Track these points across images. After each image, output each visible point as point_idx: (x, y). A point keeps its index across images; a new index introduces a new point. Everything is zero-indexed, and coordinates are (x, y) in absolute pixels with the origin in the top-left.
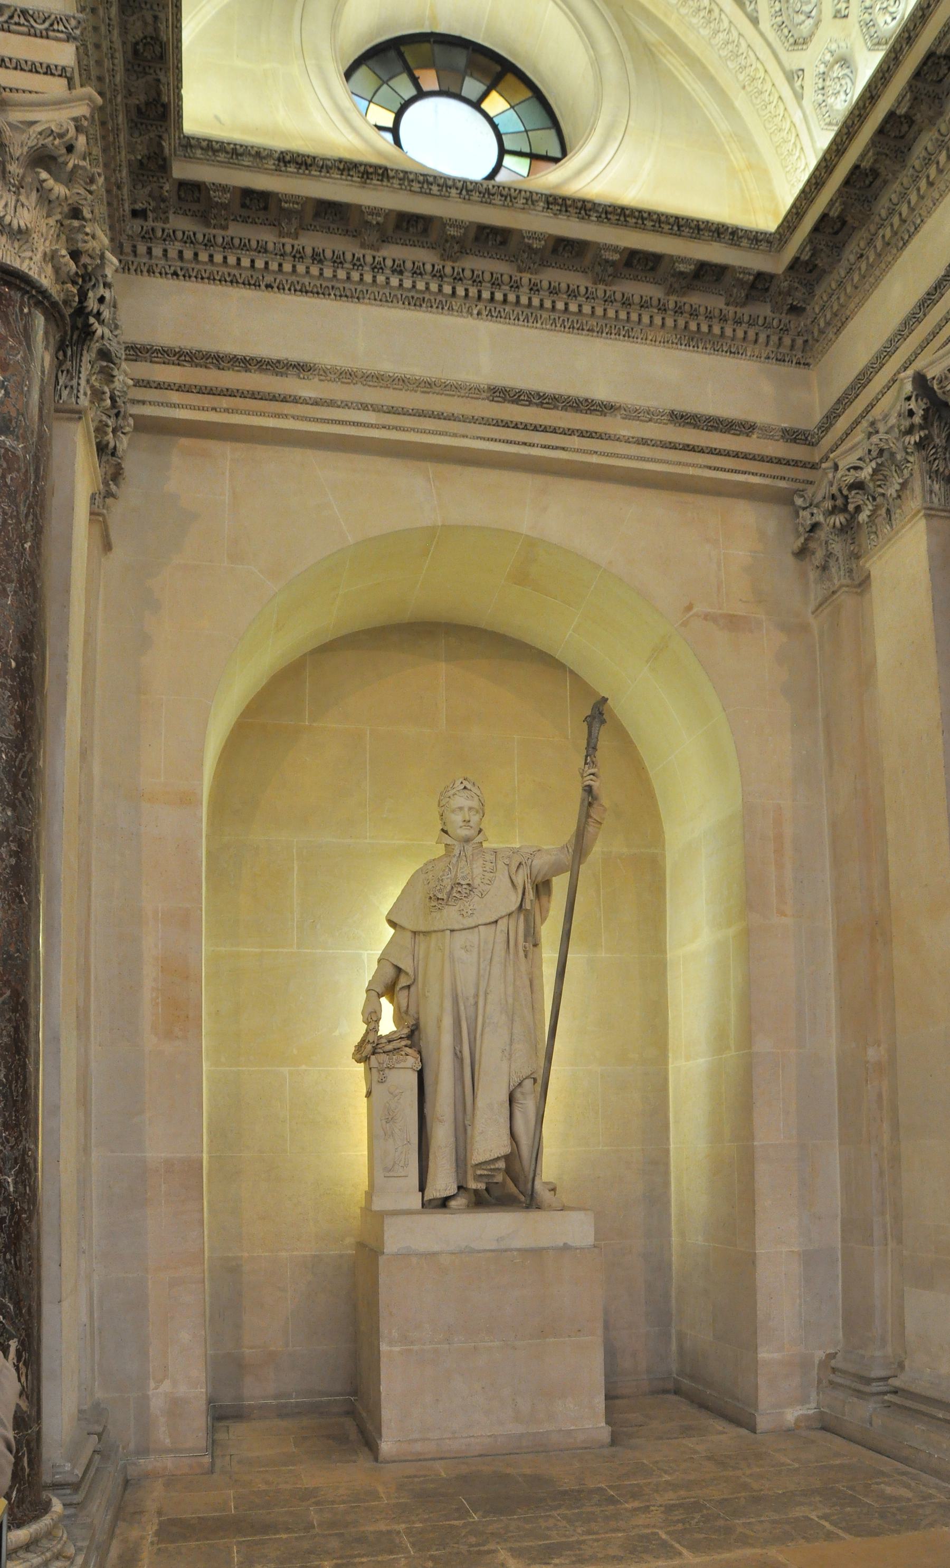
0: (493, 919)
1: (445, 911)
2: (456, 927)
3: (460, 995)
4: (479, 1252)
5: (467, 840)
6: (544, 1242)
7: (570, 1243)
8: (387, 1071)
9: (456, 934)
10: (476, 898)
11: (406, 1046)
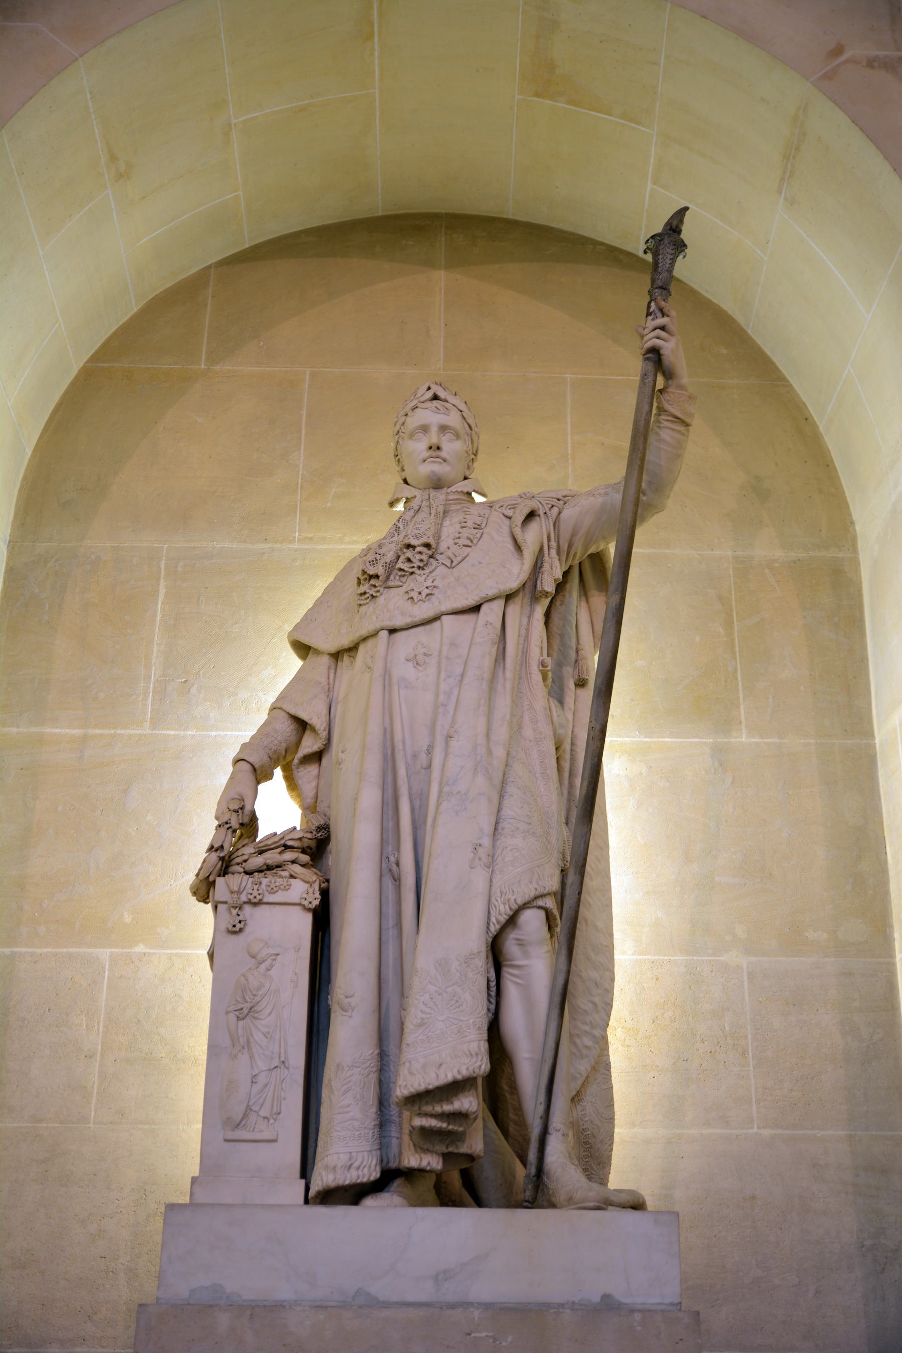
0: (471, 601)
1: (381, 600)
2: (398, 622)
3: (399, 746)
4: (387, 1305)
5: (437, 484)
6: (553, 1290)
7: (620, 1295)
8: (247, 909)
9: (398, 635)
10: (441, 570)
11: (293, 862)
